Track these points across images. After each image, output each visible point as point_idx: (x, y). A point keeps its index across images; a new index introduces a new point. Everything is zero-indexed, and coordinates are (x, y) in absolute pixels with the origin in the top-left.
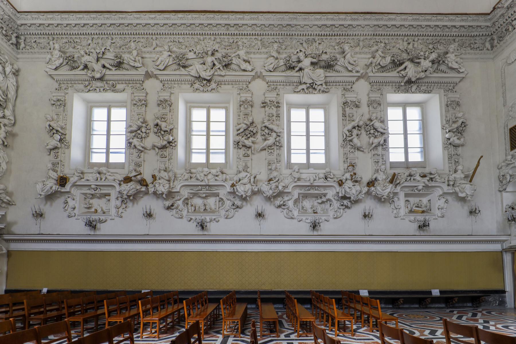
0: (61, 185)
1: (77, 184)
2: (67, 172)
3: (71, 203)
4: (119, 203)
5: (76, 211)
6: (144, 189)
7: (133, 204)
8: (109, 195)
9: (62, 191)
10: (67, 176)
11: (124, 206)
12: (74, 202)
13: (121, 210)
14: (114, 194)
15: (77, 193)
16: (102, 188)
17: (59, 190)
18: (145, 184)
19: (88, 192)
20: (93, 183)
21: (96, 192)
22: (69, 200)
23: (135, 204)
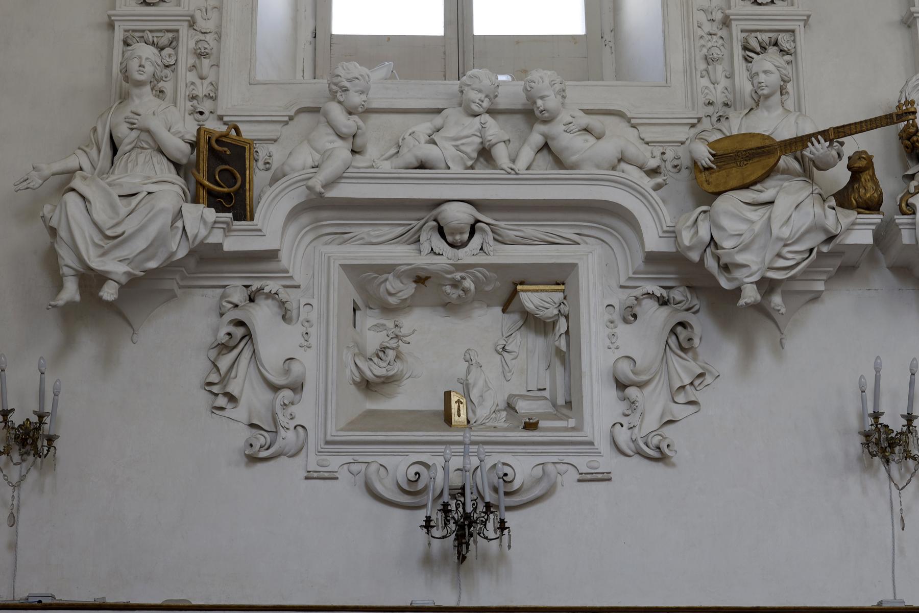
0: (217, 201)
1: (345, 191)
2: (242, 103)
3: (275, 341)
4: (643, 342)
5: (305, 411)
6: (861, 232)
7: (748, 350)
8: (560, 277)
9: (231, 244)
10: (248, 131)
11: (682, 369)
12: (294, 332)
13: (654, 402)
14: (600, 274)
15: (313, 263)
16: (506, 226)
17: (216, 237)
18: (869, 194)
19: (402, 254)
20: (457, 192)
21: (466, 255)
22: (262, 316)
23: (764, 357)
